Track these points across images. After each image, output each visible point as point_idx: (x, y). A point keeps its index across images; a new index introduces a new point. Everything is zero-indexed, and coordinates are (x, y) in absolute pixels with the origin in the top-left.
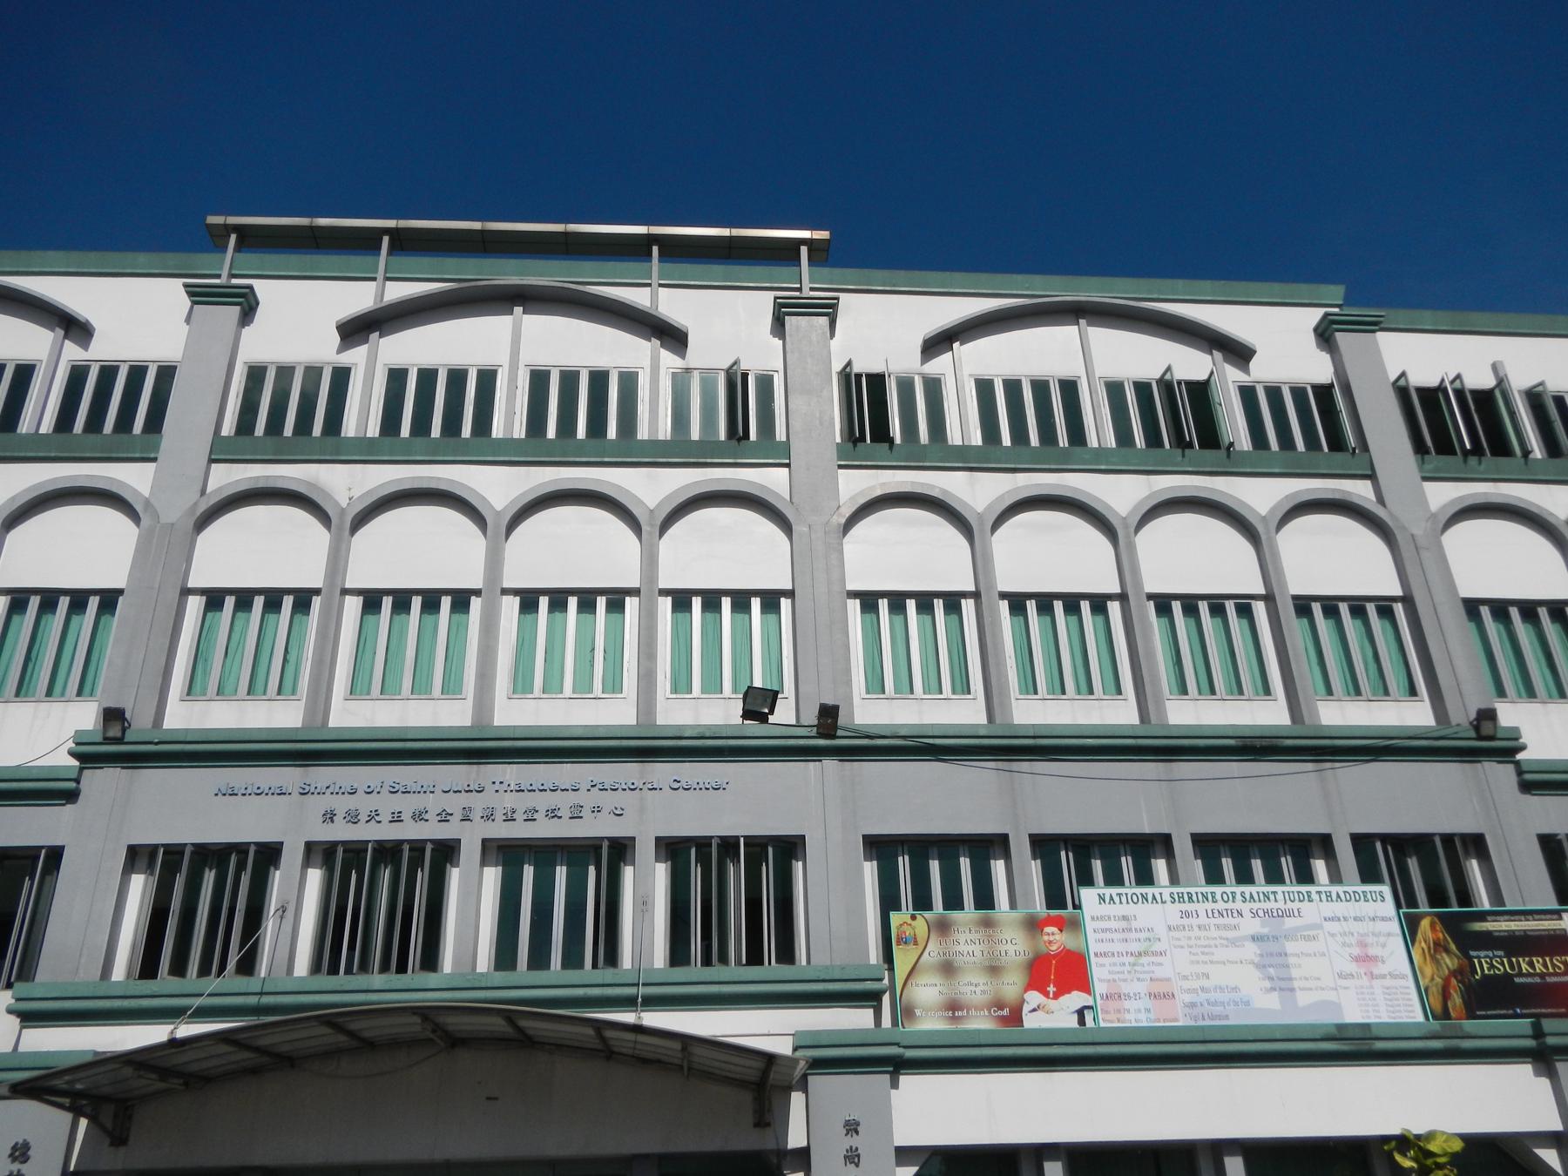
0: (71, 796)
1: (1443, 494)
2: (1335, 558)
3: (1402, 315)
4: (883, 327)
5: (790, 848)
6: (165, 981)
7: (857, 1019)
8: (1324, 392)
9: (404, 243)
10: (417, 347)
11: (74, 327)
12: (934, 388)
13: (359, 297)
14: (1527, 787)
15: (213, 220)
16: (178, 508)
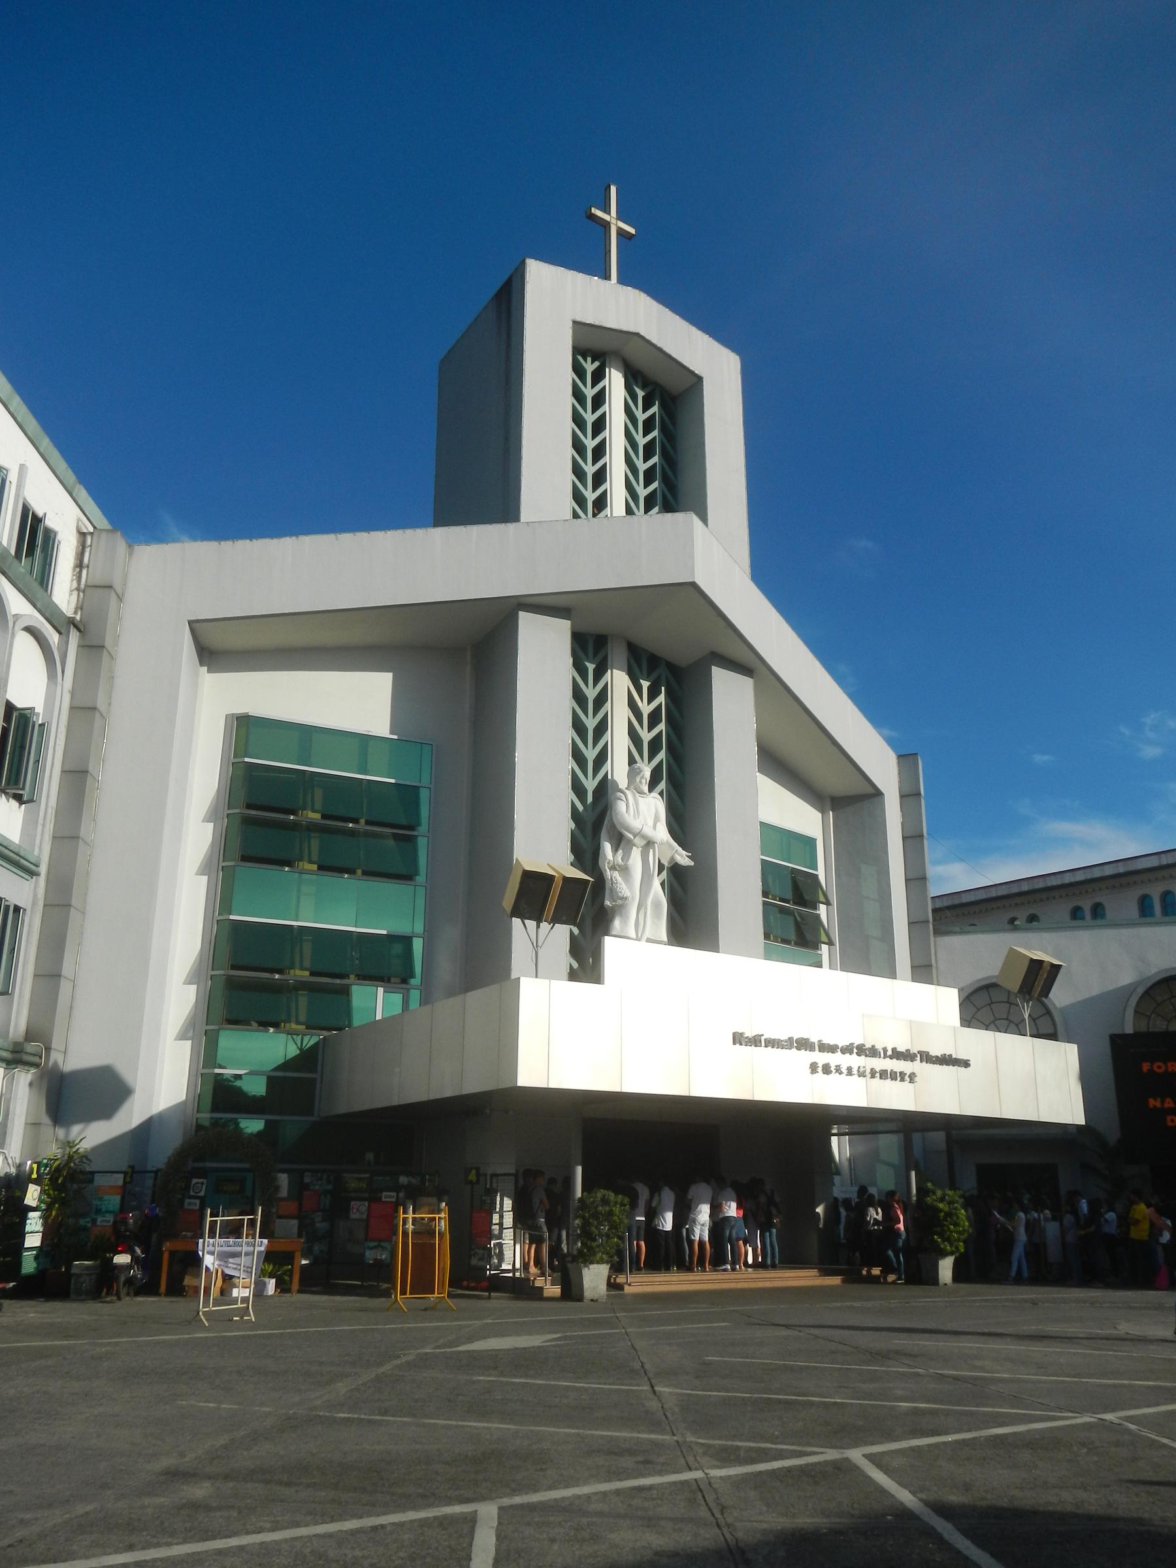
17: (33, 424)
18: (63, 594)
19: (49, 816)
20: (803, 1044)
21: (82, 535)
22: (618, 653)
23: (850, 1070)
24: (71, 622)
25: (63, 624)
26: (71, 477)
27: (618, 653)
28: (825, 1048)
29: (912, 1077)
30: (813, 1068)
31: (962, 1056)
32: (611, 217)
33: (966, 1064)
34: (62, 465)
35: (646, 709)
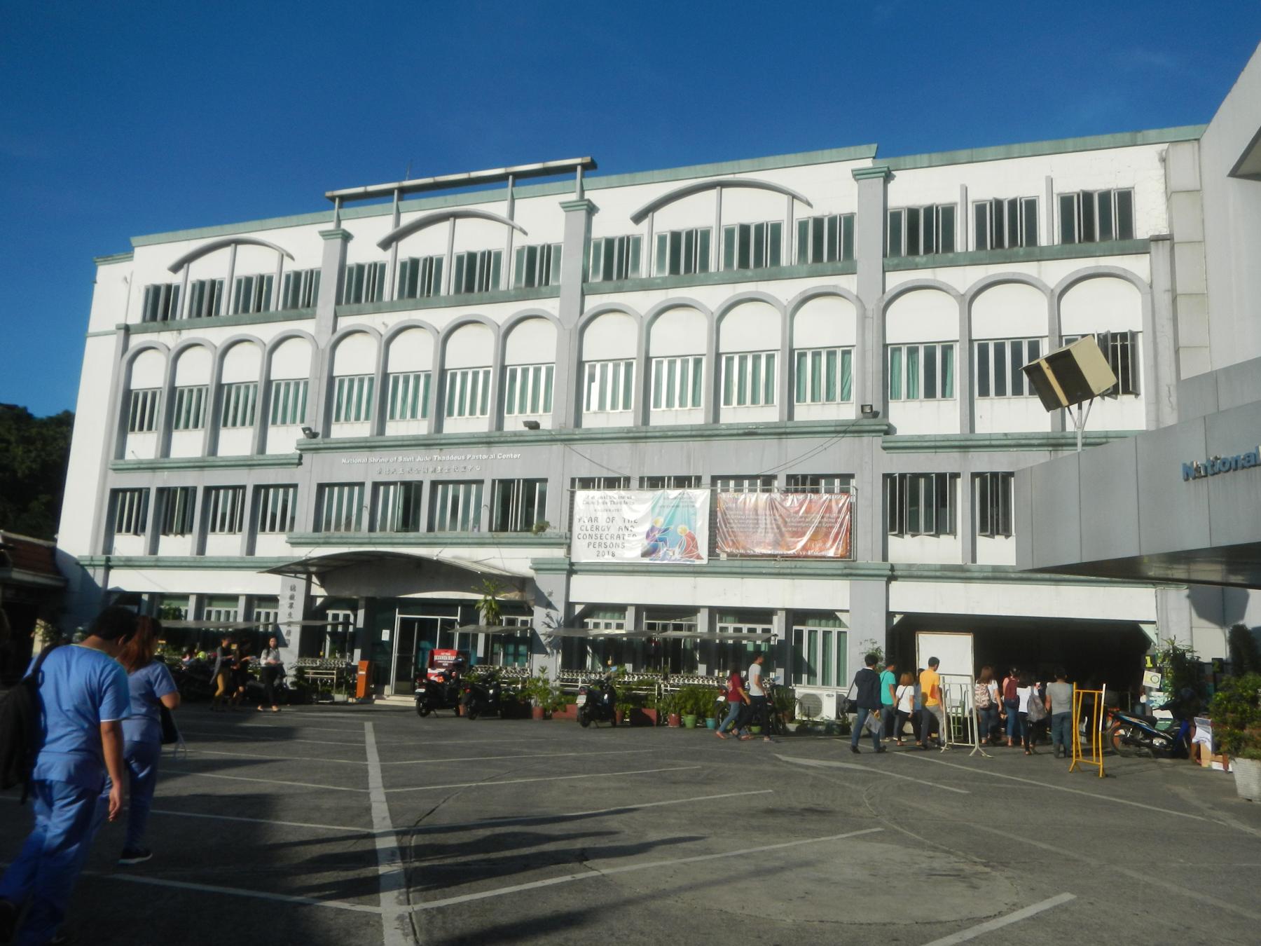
0: (300, 464)
1: (896, 280)
2: (829, 324)
3: (908, 160)
4: (617, 205)
5: (544, 481)
6: (323, 534)
7: (559, 553)
8: (849, 220)
9: (404, 192)
10: (412, 248)
11: (284, 255)
12: (637, 241)
13: (383, 225)
14: (885, 448)
15: (329, 194)
16: (326, 340)
17: (1046, 145)
18: (1149, 218)
21: (1163, 160)
24: (1157, 239)
25: (1143, 248)
26: (1127, 136)
34: (1107, 138)
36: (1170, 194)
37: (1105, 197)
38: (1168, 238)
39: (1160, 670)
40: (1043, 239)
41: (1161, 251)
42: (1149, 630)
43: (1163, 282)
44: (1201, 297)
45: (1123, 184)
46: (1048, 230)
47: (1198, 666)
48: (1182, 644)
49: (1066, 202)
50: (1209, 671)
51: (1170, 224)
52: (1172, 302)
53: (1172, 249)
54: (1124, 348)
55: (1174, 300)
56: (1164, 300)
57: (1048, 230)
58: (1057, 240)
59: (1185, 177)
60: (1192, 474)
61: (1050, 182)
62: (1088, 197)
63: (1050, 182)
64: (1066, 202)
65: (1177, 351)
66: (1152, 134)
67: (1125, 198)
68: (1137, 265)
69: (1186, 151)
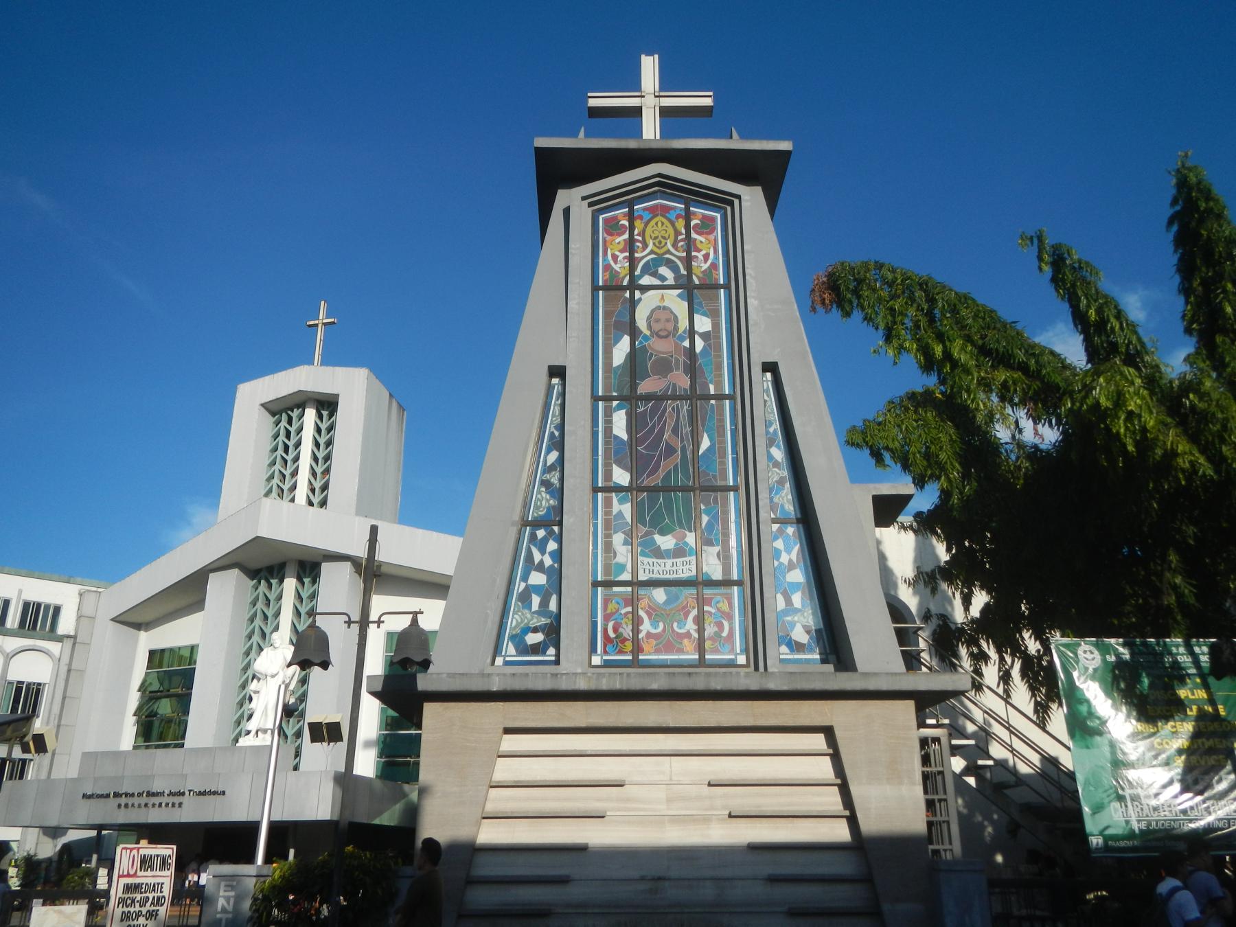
18: (66, 625)
19: (52, 718)
20: (116, 795)
21: (81, 595)
22: (291, 569)
23: (139, 806)
24: (68, 637)
25: (60, 639)
27: (291, 569)
28: (126, 795)
29: (180, 805)
30: (119, 806)
31: (220, 789)
32: (322, 317)
33: (224, 793)
35: (305, 595)
36: (79, 617)
37: (47, 607)
38: (75, 637)
39: (15, 866)
40: (9, 624)
41: (68, 643)
42: (14, 845)
43: (65, 660)
44: (82, 672)
45: (58, 602)
46: (12, 620)
47: (40, 862)
48: (32, 853)
49: (26, 605)
50: (44, 865)
51: (77, 629)
52: (70, 673)
53: (74, 644)
54: (38, 691)
55: (69, 671)
56: (64, 669)
57: (12, 620)
58: (16, 625)
59: (88, 610)
60: (85, 796)
61: (20, 592)
62: (39, 605)
63: (20, 592)
64: (26, 605)
65: (64, 698)
66: (79, 579)
67: (57, 610)
68: (54, 647)
69: (93, 597)
